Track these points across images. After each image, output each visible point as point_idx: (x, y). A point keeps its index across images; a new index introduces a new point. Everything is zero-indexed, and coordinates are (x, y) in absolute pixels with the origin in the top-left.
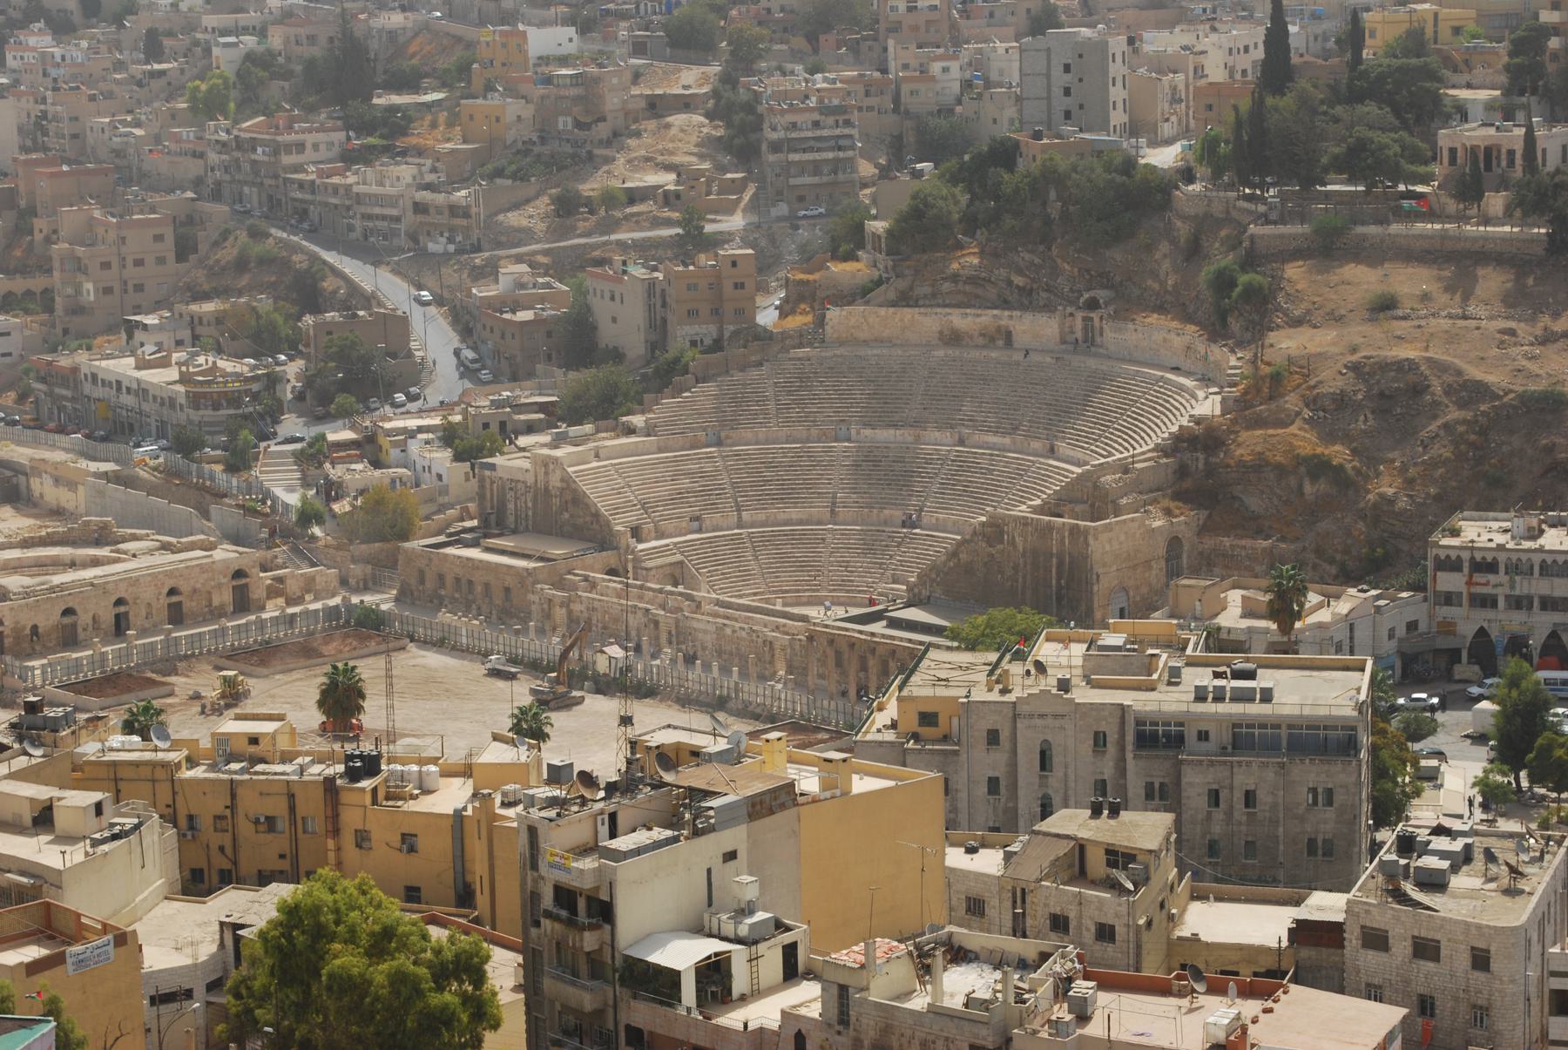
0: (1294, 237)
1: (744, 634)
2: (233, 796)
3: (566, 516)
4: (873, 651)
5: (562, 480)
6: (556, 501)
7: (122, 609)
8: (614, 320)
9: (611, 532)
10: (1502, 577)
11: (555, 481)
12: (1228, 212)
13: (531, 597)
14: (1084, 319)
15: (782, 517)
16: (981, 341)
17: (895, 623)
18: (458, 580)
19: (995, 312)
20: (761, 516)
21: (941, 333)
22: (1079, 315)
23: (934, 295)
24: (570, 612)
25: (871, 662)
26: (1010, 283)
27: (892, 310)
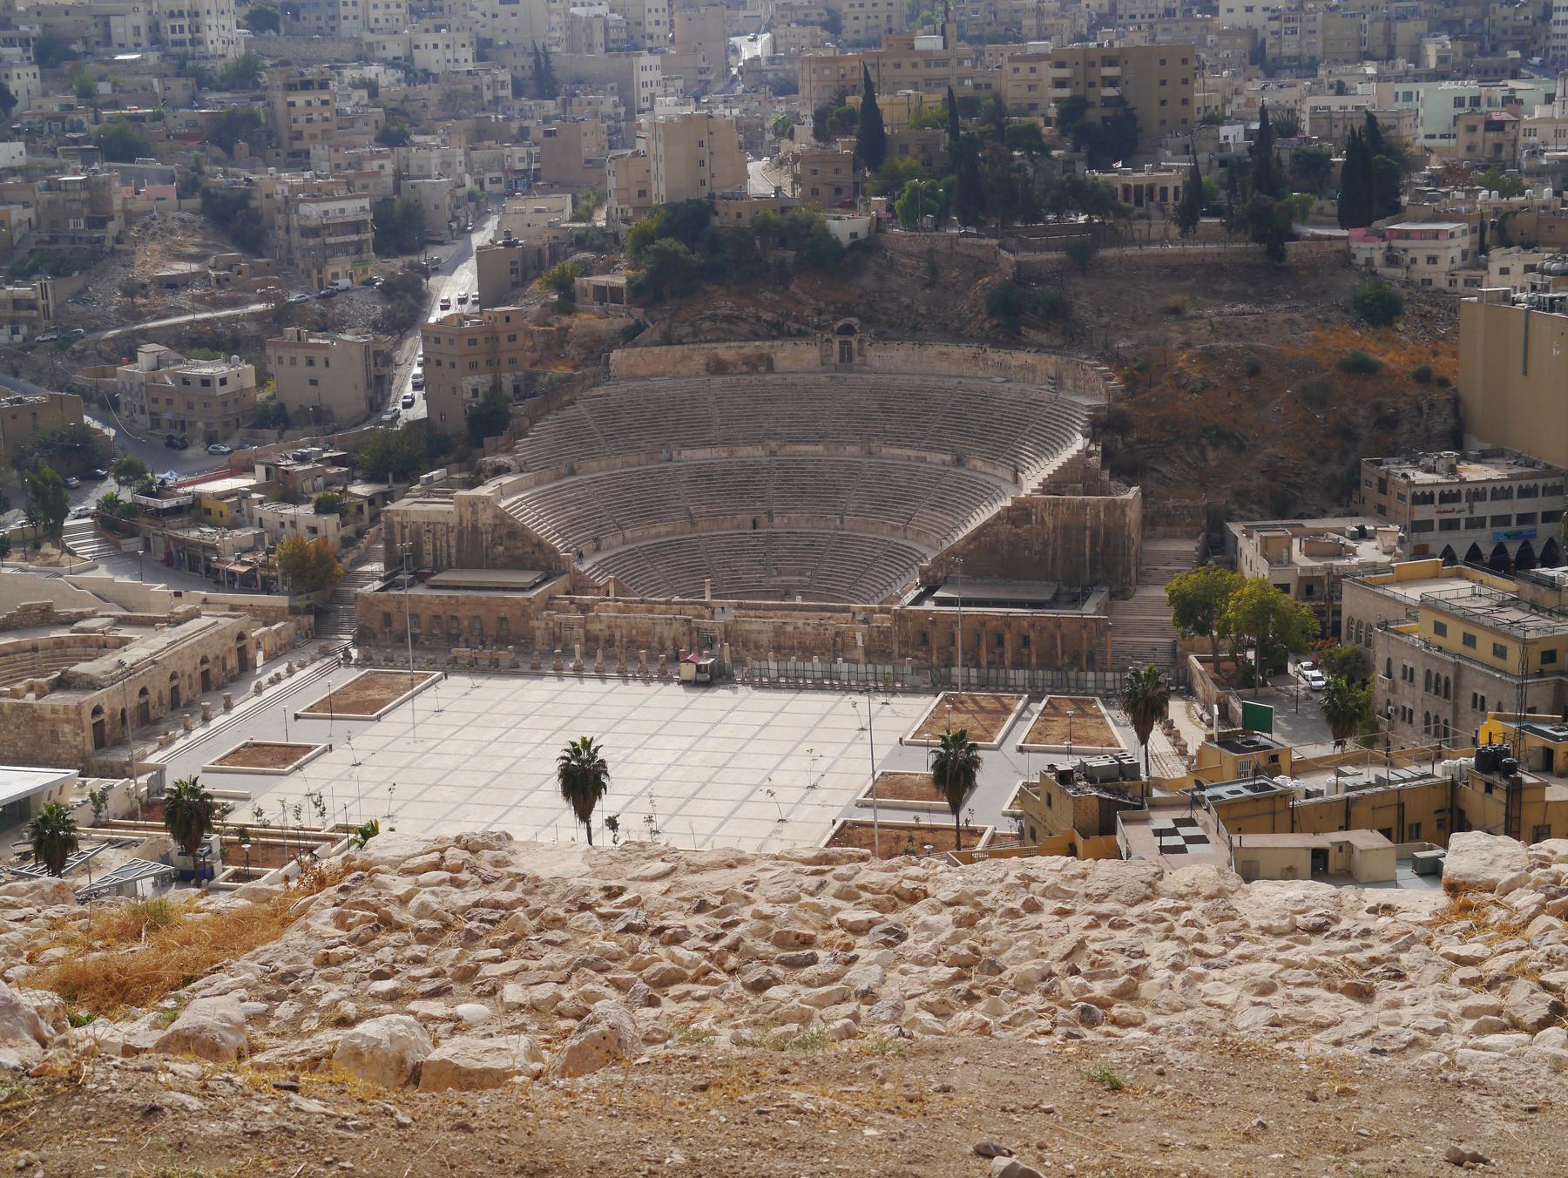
0: (1051, 262)
1: (809, 629)
2: (1293, 822)
3: (501, 549)
4: (1009, 625)
5: (495, 517)
6: (487, 539)
7: (175, 682)
8: (314, 382)
9: (558, 559)
10: (1464, 504)
11: (486, 518)
13: (534, 623)
15: (653, 531)
16: (744, 369)
17: (941, 602)
18: (437, 617)
20: (638, 533)
21: (708, 365)
23: (695, 334)
24: (587, 632)
25: (1007, 636)
26: (759, 319)
27: (664, 348)
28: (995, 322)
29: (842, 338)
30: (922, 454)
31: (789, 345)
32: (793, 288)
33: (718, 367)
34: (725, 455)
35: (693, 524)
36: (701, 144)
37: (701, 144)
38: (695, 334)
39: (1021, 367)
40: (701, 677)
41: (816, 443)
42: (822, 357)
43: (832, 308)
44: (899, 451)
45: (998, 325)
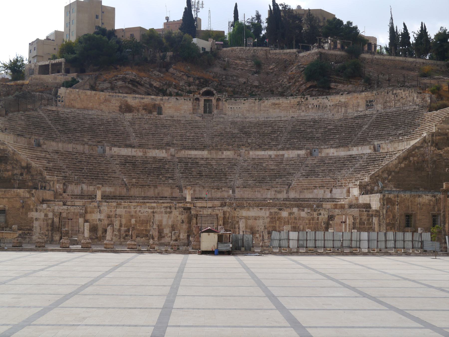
12: (267, 55)
13: (33, 215)
14: (205, 100)
19: (153, 97)
21: (120, 107)
22: (202, 99)
26: (151, 85)
27: (94, 92)
28: (309, 85)
29: (206, 98)
30: (281, 152)
31: (173, 99)
32: (171, 70)
33: (128, 109)
34: (140, 154)
35: (128, 190)
36: (97, 17)
37: (97, 17)
38: (113, 88)
39: (336, 105)
40: (223, 247)
41: (203, 149)
42: (193, 109)
43: (197, 82)
44: (262, 153)
45: (310, 87)
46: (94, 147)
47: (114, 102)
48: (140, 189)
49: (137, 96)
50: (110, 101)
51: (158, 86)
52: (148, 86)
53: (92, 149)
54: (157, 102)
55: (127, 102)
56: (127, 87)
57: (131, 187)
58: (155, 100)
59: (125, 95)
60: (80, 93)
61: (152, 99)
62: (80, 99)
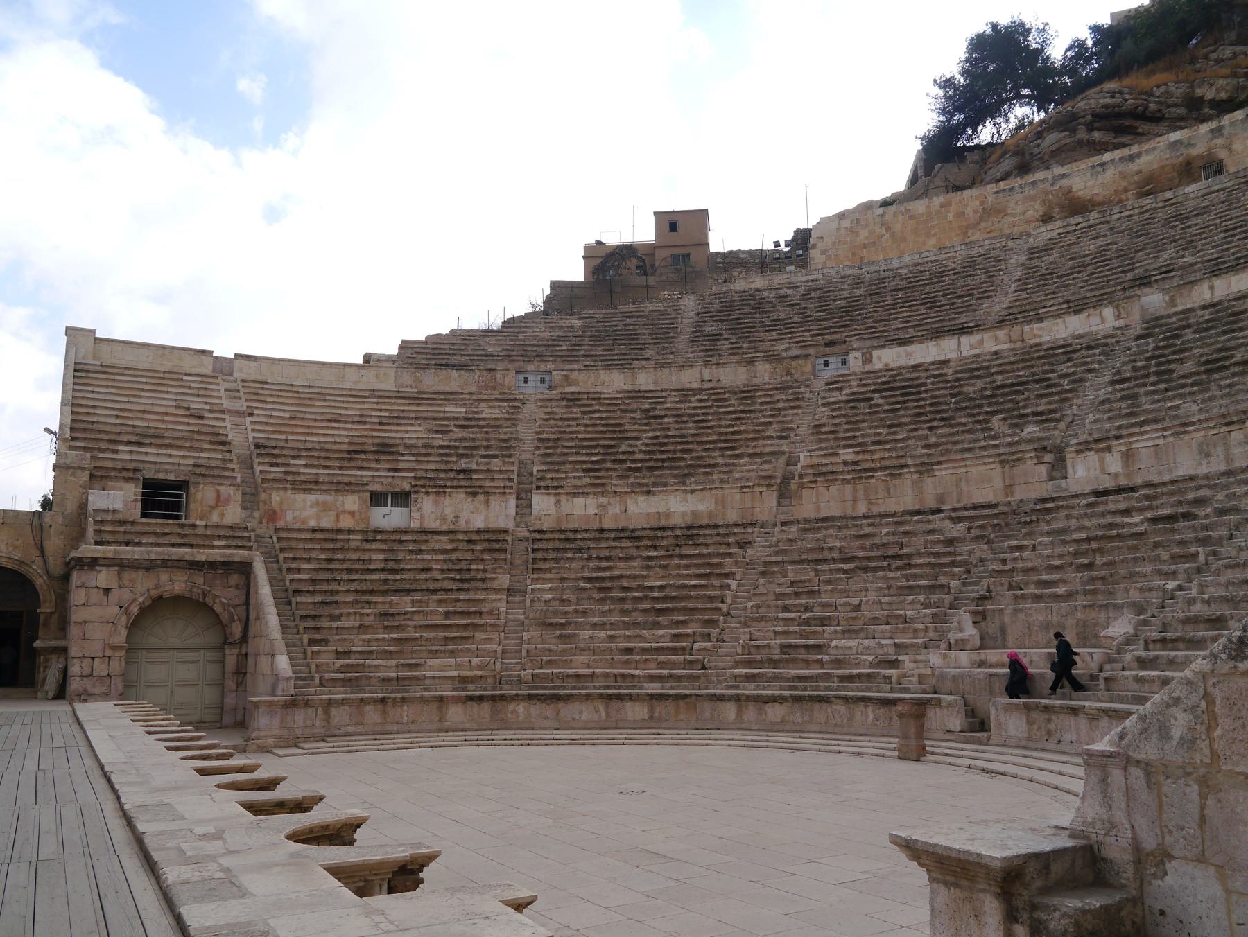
19: (1175, 136)
46: (794, 363)
47: (1019, 209)
48: (849, 488)
49: (1107, 157)
50: (1001, 212)
51: (1224, 95)
52: (1182, 111)
53: (789, 373)
54: (1198, 150)
55: (1070, 191)
56: (1080, 143)
57: (801, 485)
58: (1190, 145)
59: (1058, 170)
60: (887, 217)
61: (1176, 142)
62: (893, 235)
